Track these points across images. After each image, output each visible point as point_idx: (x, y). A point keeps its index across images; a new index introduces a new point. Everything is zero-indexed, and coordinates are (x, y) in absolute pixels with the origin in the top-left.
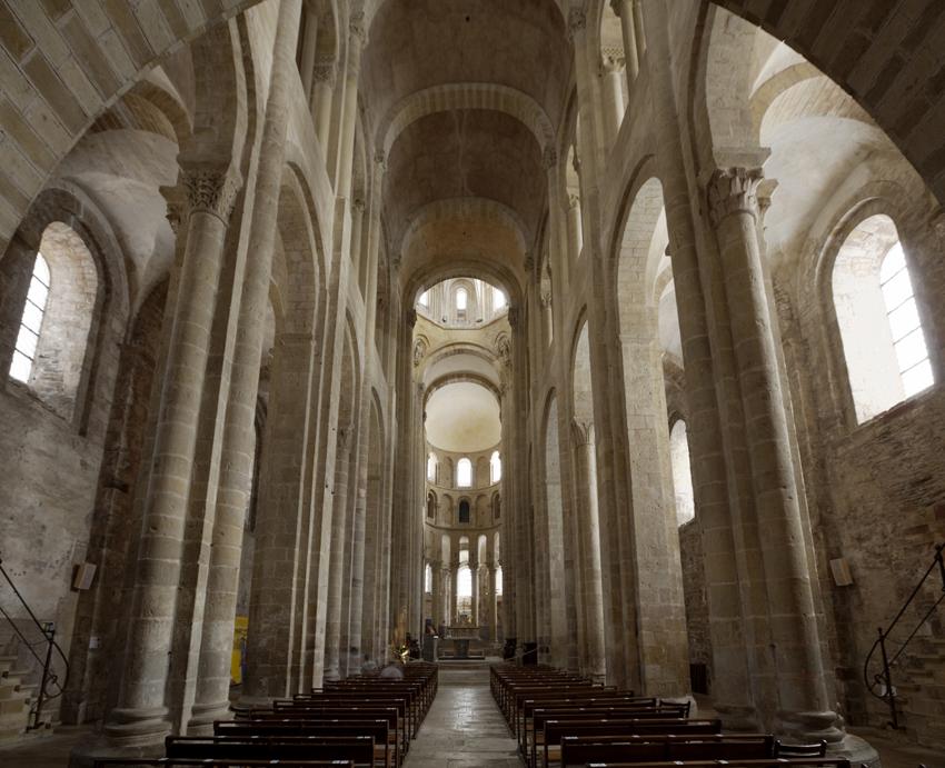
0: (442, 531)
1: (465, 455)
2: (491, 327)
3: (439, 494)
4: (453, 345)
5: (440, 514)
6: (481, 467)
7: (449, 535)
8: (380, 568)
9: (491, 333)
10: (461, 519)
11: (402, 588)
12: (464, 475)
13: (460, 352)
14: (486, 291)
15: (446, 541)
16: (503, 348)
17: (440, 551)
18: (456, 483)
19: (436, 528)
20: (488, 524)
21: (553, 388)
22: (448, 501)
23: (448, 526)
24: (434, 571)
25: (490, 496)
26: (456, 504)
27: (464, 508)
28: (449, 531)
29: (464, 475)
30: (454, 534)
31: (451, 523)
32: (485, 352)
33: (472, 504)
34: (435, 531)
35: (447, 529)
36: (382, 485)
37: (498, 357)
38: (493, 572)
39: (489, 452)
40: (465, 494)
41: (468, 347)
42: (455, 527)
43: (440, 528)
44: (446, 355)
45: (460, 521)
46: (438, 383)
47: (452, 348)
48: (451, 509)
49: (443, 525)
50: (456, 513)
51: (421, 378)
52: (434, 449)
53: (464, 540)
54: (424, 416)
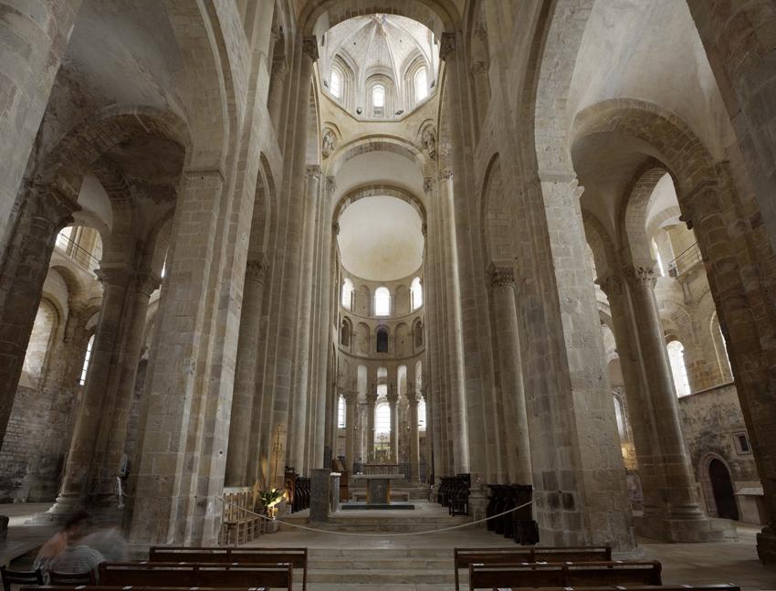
0: (358, 360)
1: (383, 284)
2: (415, 115)
3: (355, 321)
5: (356, 343)
6: (400, 294)
7: (367, 366)
8: (207, 330)
9: (412, 124)
11: (279, 394)
12: (382, 304)
13: (377, 147)
14: (407, 84)
15: (362, 373)
16: (428, 139)
17: (355, 382)
18: (373, 313)
19: (352, 356)
20: (408, 353)
21: (496, 155)
23: (366, 356)
25: (410, 324)
26: (373, 333)
27: (382, 338)
29: (382, 304)
30: (372, 365)
32: (406, 145)
33: (391, 333)
34: (349, 359)
35: (364, 359)
36: (226, 188)
37: (421, 151)
38: (414, 404)
39: (410, 279)
41: (387, 140)
43: (355, 357)
44: (361, 150)
45: (378, 351)
46: (354, 194)
47: (367, 141)
48: (368, 338)
51: (330, 170)
52: (349, 276)
53: (382, 373)
54: (335, 228)
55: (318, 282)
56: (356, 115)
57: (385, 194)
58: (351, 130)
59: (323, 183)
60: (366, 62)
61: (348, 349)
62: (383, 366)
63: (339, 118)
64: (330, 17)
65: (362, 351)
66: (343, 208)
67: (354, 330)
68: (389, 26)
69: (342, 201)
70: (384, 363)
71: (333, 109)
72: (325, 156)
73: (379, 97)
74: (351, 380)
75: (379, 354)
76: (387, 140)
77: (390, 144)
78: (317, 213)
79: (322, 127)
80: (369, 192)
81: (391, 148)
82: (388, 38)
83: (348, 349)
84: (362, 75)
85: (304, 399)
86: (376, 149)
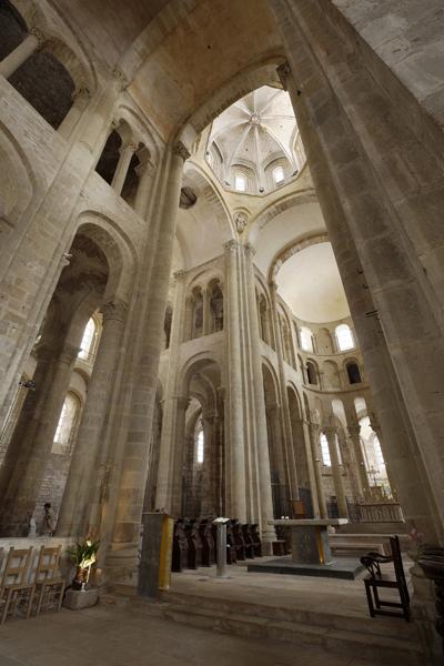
0: (330, 396)
3: (320, 361)
4: (273, 203)
10: (352, 382)
13: (284, 207)
15: (338, 408)
18: (338, 349)
22: (332, 367)
23: (338, 390)
24: (330, 439)
26: (341, 367)
28: (338, 395)
31: (340, 386)
35: (335, 393)
40: (351, 355)
42: (346, 389)
46: (283, 255)
49: (330, 389)
50: (345, 376)
52: (305, 324)
55: (246, 326)
56: (261, 194)
57: (311, 244)
58: (257, 205)
59: (241, 250)
60: (260, 157)
61: (318, 387)
62: (360, 396)
63: (246, 202)
64: (194, 127)
65: (333, 386)
66: (276, 268)
67: (320, 368)
68: (267, 121)
69: (274, 263)
70: (359, 393)
71: (238, 198)
72: (240, 232)
73: (279, 175)
74: (327, 415)
75: (352, 386)
76: (290, 197)
77: (293, 199)
78: (238, 274)
79: (232, 214)
80: (295, 248)
81: (295, 202)
82: (270, 130)
83: (318, 387)
84: (260, 170)
85: (241, 437)
86: (283, 210)
